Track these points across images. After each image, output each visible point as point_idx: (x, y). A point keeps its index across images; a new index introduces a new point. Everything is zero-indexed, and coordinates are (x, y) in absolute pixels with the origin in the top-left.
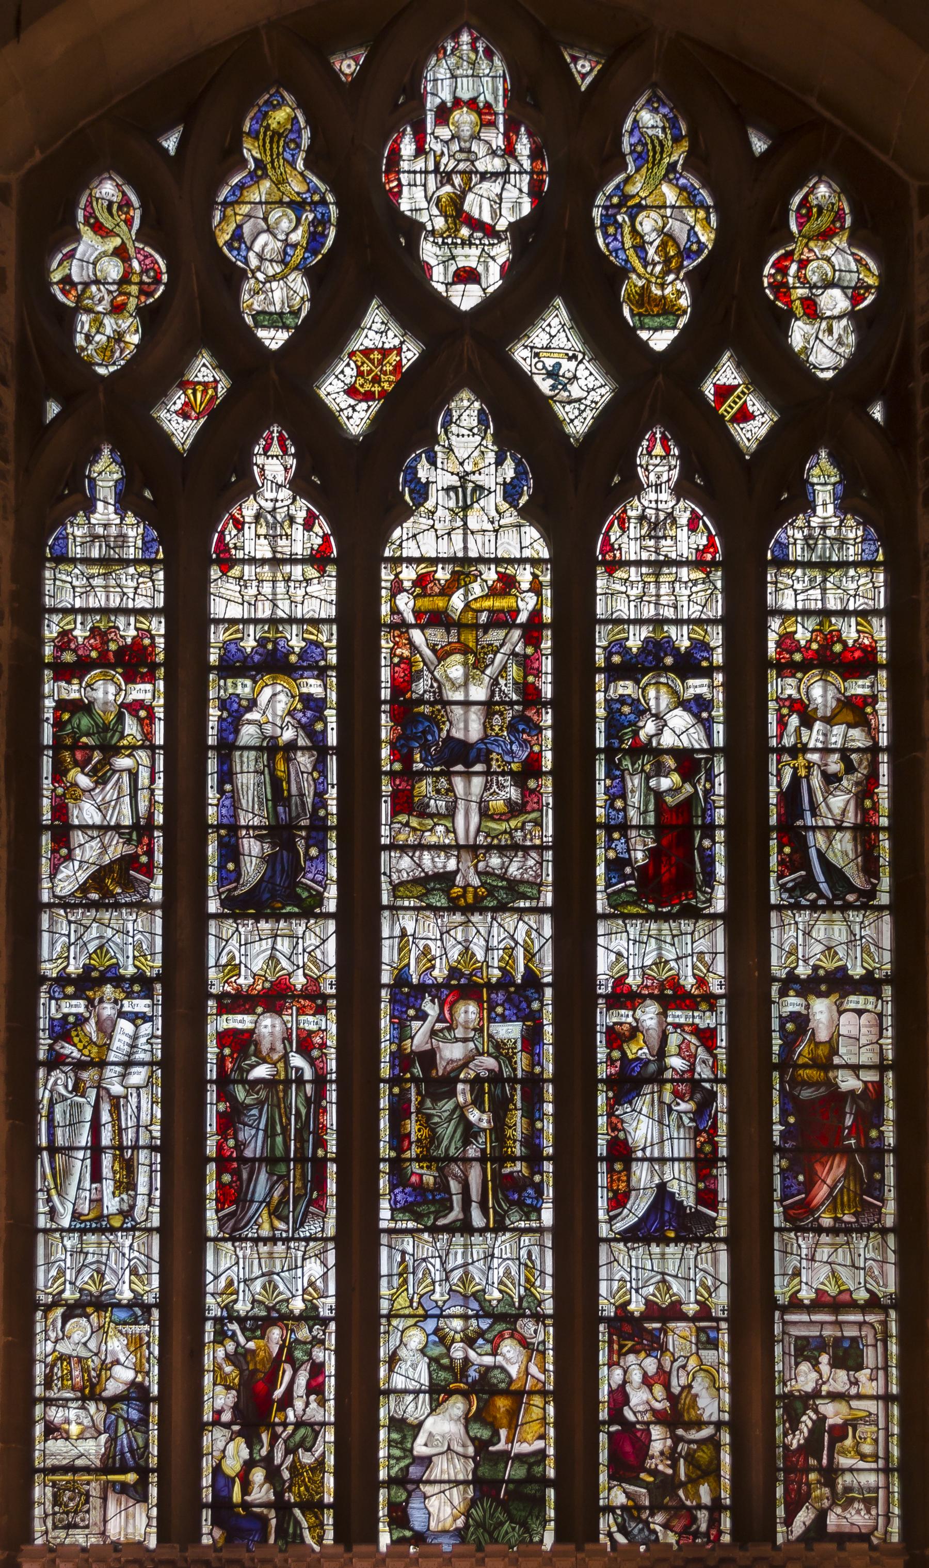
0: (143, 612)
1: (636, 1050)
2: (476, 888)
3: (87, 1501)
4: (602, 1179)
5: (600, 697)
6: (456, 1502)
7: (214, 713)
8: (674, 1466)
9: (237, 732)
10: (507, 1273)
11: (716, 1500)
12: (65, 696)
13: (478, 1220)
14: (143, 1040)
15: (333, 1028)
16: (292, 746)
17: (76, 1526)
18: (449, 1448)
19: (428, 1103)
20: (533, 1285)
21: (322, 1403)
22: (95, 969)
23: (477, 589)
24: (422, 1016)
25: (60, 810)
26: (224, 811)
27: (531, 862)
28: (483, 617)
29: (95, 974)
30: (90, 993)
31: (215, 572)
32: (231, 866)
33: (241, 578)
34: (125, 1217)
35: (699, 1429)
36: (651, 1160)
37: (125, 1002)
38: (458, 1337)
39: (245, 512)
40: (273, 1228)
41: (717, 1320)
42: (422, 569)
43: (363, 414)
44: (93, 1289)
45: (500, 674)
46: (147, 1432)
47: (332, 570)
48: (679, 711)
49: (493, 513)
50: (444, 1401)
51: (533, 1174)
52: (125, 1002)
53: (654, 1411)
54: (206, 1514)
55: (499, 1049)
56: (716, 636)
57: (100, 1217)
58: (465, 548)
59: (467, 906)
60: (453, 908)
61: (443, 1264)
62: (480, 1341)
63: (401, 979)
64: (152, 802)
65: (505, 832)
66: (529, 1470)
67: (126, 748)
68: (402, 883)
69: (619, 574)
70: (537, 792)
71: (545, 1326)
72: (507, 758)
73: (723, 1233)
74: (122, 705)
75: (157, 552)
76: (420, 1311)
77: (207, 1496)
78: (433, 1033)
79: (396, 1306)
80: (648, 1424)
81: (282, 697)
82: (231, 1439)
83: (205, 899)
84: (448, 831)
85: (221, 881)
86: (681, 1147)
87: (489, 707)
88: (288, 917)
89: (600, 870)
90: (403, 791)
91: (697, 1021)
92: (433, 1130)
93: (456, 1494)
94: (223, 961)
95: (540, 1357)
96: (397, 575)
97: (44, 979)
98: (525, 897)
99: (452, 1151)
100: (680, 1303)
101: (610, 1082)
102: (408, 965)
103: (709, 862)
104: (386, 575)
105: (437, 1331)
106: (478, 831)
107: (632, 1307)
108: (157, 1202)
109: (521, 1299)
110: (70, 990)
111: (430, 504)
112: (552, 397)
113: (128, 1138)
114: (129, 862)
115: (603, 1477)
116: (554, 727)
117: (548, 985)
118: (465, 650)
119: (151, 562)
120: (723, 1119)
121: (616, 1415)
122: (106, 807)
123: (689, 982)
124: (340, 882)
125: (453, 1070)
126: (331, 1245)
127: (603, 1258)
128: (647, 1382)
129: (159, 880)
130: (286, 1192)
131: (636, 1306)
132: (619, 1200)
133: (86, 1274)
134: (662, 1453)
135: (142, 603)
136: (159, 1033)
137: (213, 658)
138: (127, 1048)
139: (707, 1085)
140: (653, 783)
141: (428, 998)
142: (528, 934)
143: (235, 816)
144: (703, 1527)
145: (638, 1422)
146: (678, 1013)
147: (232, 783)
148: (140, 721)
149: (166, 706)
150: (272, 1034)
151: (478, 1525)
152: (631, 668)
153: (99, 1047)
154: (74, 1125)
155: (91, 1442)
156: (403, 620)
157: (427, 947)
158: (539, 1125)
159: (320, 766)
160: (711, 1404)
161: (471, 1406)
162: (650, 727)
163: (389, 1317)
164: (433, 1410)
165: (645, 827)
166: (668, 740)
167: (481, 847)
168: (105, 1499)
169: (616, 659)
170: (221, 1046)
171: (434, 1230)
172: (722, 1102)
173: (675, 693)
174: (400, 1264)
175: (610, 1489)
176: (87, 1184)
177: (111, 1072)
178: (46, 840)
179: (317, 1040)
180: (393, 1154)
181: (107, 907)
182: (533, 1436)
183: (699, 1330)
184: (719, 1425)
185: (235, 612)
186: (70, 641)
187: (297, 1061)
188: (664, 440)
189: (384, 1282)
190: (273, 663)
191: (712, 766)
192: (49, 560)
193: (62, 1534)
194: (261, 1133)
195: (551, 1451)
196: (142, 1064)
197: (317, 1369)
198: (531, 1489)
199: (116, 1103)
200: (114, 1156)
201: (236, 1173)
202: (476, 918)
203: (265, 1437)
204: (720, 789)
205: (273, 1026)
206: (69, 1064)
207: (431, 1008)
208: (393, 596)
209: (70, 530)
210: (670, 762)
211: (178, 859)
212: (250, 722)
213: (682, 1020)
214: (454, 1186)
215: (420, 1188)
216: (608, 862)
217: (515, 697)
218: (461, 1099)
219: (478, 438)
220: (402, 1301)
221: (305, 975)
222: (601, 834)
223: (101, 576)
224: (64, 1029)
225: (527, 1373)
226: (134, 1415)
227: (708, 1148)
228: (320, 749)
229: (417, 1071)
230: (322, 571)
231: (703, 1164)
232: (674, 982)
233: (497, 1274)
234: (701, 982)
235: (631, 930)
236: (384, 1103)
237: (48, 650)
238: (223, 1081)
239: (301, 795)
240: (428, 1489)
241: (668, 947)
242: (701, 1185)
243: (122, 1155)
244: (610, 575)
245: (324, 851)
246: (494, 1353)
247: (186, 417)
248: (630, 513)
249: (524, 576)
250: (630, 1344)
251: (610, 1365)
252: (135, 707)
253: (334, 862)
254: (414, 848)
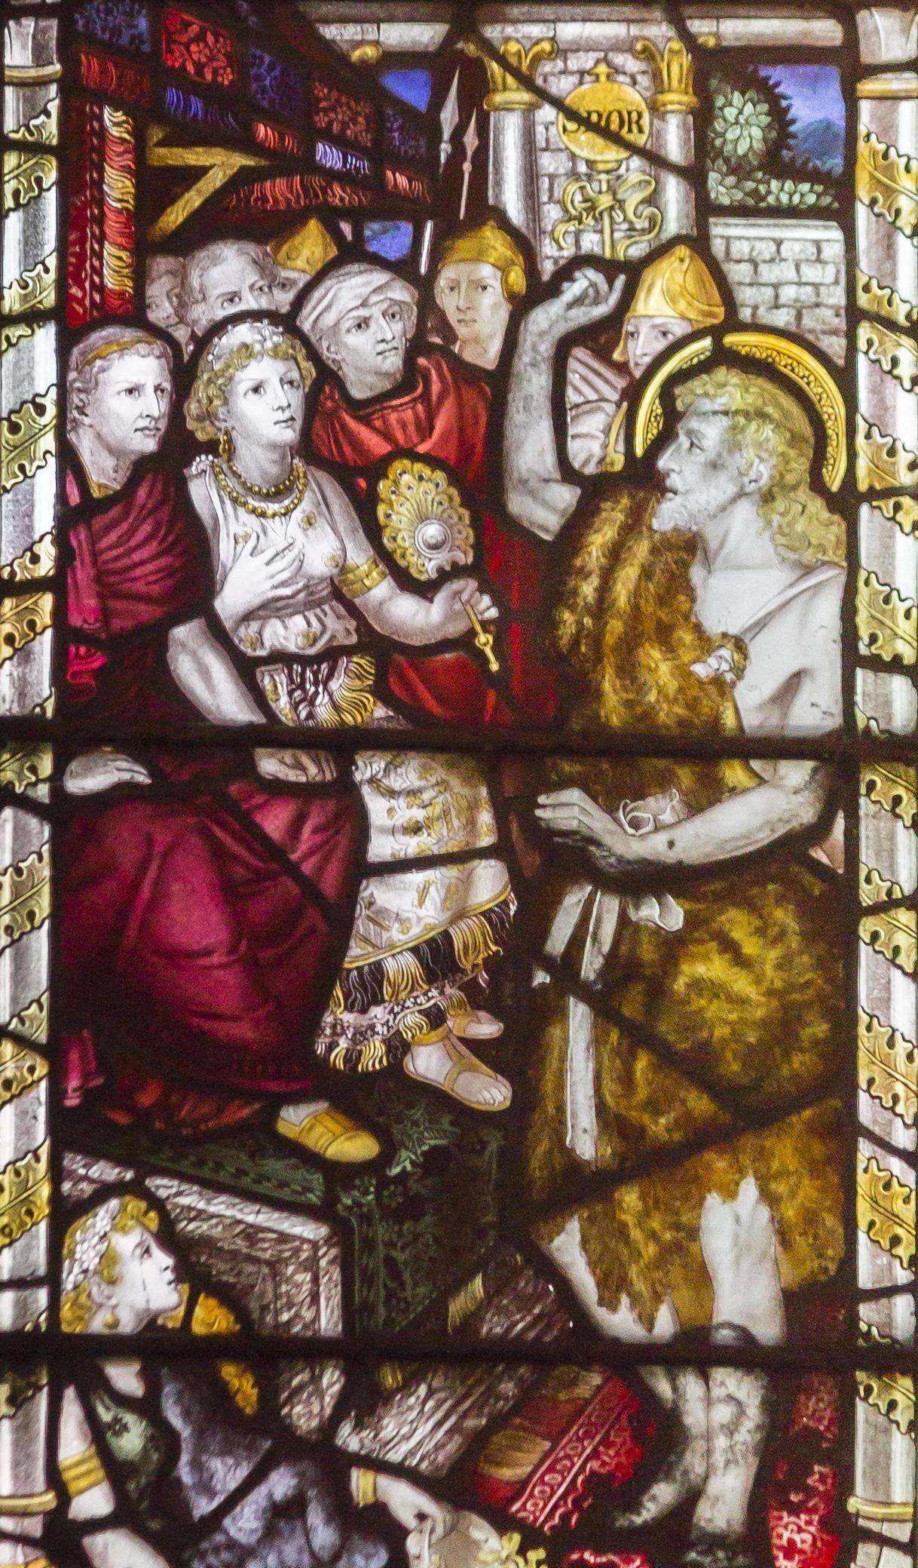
8: (521, 1055)
35: (707, 794)
53: (384, 654)
80: (342, 744)
128: (339, 444)
134: (437, 957)
144: (725, 1502)
145: (273, 734)
175: (66, 1214)
250: (220, 165)
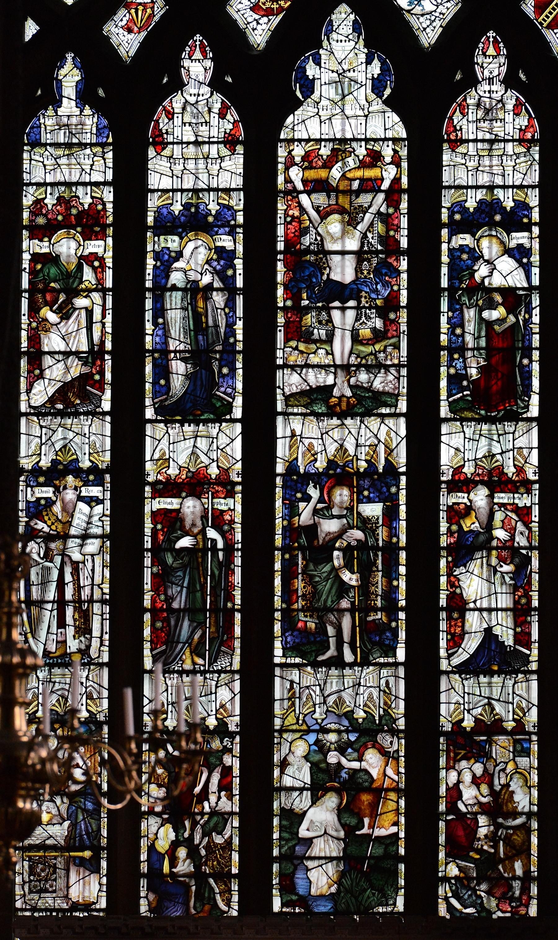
0: (97, 184)
1: (470, 524)
2: (348, 398)
3: (55, 872)
4: (443, 626)
5: (444, 247)
6: (330, 874)
7: (150, 262)
8: (496, 847)
9: (168, 277)
10: (370, 697)
11: (527, 871)
12: (38, 250)
13: (348, 657)
14: (96, 518)
15: (239, 508)
16: (210, 287)
17: (46, 891)
18: (325, 832)
19: (311, 567)
20: (390, 707)
21: (230, 797)
22: (60, 463)
23: (351, 162)
24: (307, 498)
25: (35, 339)
26: (158, 339)
27: (391, 377)
28: (356, 185)
29: (60, 467)
30: (57, 482)
31: (151, 152)
32: (162, 382)
33: (171, 157)
34: (83, 655)
35: (514, 819)
36: (481, 610)
37: (83, 489)
38: (332, 747)
39: (174, 105)
40: (194, 663)
41: (530, 734)
42: (309, 147)
43: (264, 26)
44: (59, 710)
45: (368, 230)
46: (99, 819)
47: (240, 149)
48: (506, 257)
49: (363, 102)
50: (323, 796)
51: (390, 621)
52: (83, 489)
53: (480, 803)
54: (143, 882)
55: (365, 524)
56: (533, 199)
57: (65, 654)
58: (343, 130)
59: (343, 411)
60: (330, 414)
61: (321, 690)
62: (350, 750)
63: (292, 467)
64: (103, 333)
65: (371, 354)
66: (385, 849)
67: (84, 291)
68: (292, 395)
69: (462, 149)
70: (396, 322)
71: (399, 739)
72: (373, 296)
73: (534, 666)
74: (81, 257)
75: (108, 137)
76: (304, 727)
77: (144, 868)
78: (315, 512)
79: (286, 723)
80: (476, 814)
81: (202, 250)
82: (162, 825)
83: (143, 407)
84: (327, 353)
85: (155, 394)
86: (505, 601)
87: (360, 255)
88: (206, 422)
89: (443, 384)
90: (294, 322)
91: (516, 501)
92: (314, 587)
93: (330, 868)
94: (156, 456)
95: (394, 762)
96: (290, 152)
97: (22, 471)
98: (386, 405)
99: (329, 603)
100: (501, 720)
101: (449, 548)
102: (296, 459)
103: (528, 376)
104: (282, 152)
105: (317, 742)
106: (351, 353)
107: (464, 724)
108: (107, 643)
109: (380, 717)
110: (42, 479)
111: (316, 96)
112: (409, 11)
113: (85, 593)
114: (84, 379)
115: (442, 855)
116: (408, 271)
117: (403, 474)
118: (341, 211)
119: (103, 145)
120: (536, 577)
121: (452, 808)
122: (67, 338)
123: (510, 470)
124: (245, 394)
125: (330, 540)
126: (237, 677)
127: (443, 687)
128: (476, 781)
129: (108, 394)
130: (203, 635)
131: (468, 723)
132: (456, 641)
133: (54, 698)
134: (486, 836)
135: (97, 177)
136: (108, 513)
137: (150, 220)
138: (84, 525)
139: (524, 552)
140: (486, 314)
141: (311, 485)
142: (388, 434)
143: (166, 343)
144: (517, 893)
145: (469, 813)
146: (502, 495)
147: (163, 317)
148: (95, 269)
149: (114, 257)
150: (193, 513)
151: (347, 891)
152: (469, 222)
153: (64, 523)
154: (44, 584)
155: (57, 827)
156: (294, 187)
157: (311, 444)
158: (395, 583)
159: (230, 304)
160: (524, 799)
161: (342, 800)
162: (482, 271)
163: (282, 731)
164: (314, 803)
165: (478, 349)
166: (497, 281)
167: (354, 365)
168: (68, 871)
169: (457, 217)
170: (154, 522)
171: (316, 665)
172: (535, 563)
173: (502, 243)
174: (289, 691)
175: (447, 864)
176: (54, 629)
177: (72, 543)
178: (24, 363)
179: (227, 517)
180: (284, 606)
181: (69, 415)
182: (389, 823)
183: (516, 742)
184: (529, 815)
185: (166, 183)
186: (42, 207)
187: (212, 533)
188: (496, 42)
189: (277, 705)
190: (194, 222)
191: (530, 302)
192: (26, 145)
193: (36, 897)
194: (185, 590)
195: (402, 835)
196: (96, 537)
197: (227, 771)
198: (387, 864)
199: (76, 566)
200: (75, 607)
201: (166, 620)
202: (349, 421)
203: (187, 823)
204: (536, 319)
205: (194, 507)
206: (40, 537)
207: (314, 492)
208: (287, 169)
209: (42, 121)
210: (498, 298)
211: (123, 377)
212: (177, 270)
213: (505, 501)
214: (331, 631)
215: (305, 631)
216: (449, 376)
217: (380, 248)
218: (336, 563)
219: (352, 43)
220: (291, 719)
221: (218, 467)
222: (444, 354)
223: (65, 157)
224: (39, 509)
225: (385, 775)
226: (90, 806)
227: (523, 601)
228: (230, 289)
229: (303, 541)
230: (233, 151)
231: (520, 613)
232: (500, 470)
233: (361, 700)
234: (520, 470)
235: (466, 430)
236: (278, 566)
237: (26, 215)
238: (156, 550)
239: (216, 326)
240: (310, 864)
241: (494, 443)
242: (519, 630)
243: (80, 607)
244: (453, 151)
245: (233, 370)
246: (360, 759)
247: (130, 31)
248: (468, 101)
249: (388, 152)
250: (463, 752)
251: (448, 769)
252: (90, 259)
253: (241, 378)
254: (302, 367)
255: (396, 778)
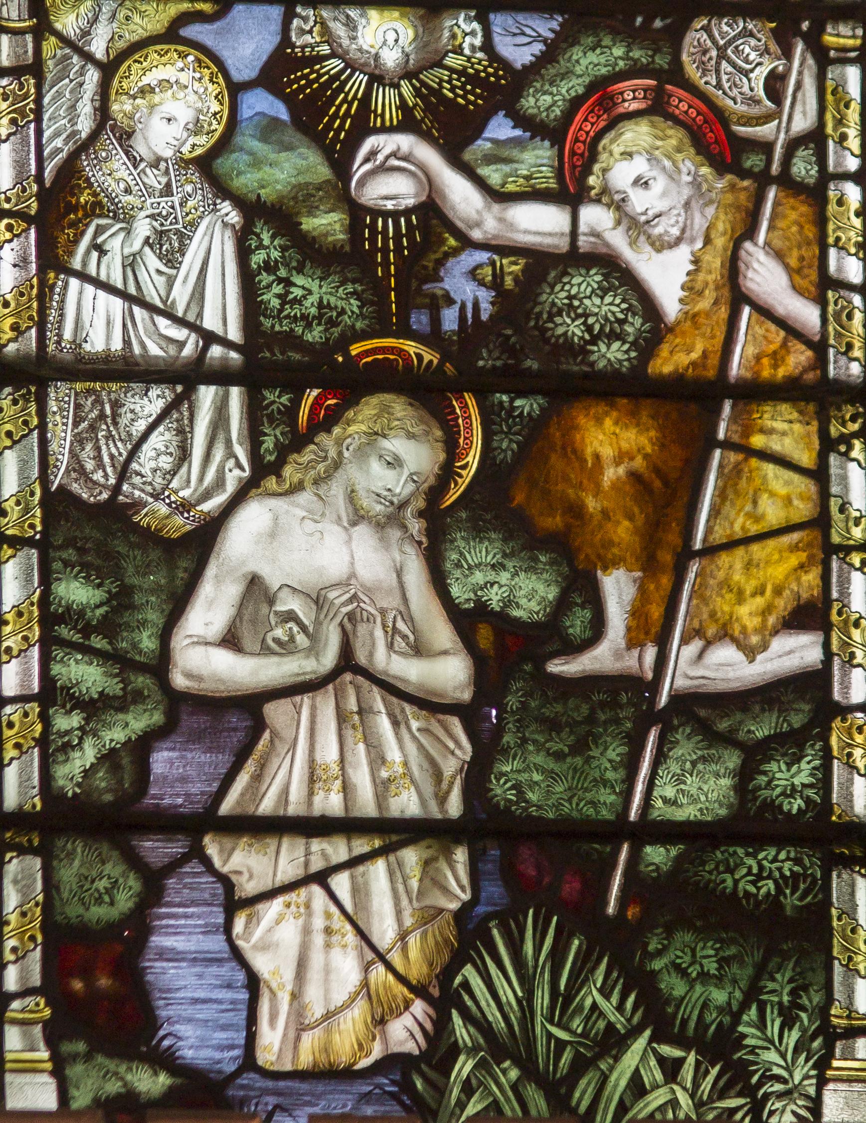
6: (385, 931)
18: (347, 662)
50: (325, 421)
66: (744, 777)
71: (824, 60)
93: (384, 893)
95: (797, 212)
105: (281, 69)
161: (452, 448)
164: (263, 473)
225: (737, 296)
240: (249, 864)
255: (808, 315)
